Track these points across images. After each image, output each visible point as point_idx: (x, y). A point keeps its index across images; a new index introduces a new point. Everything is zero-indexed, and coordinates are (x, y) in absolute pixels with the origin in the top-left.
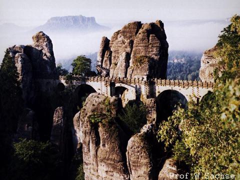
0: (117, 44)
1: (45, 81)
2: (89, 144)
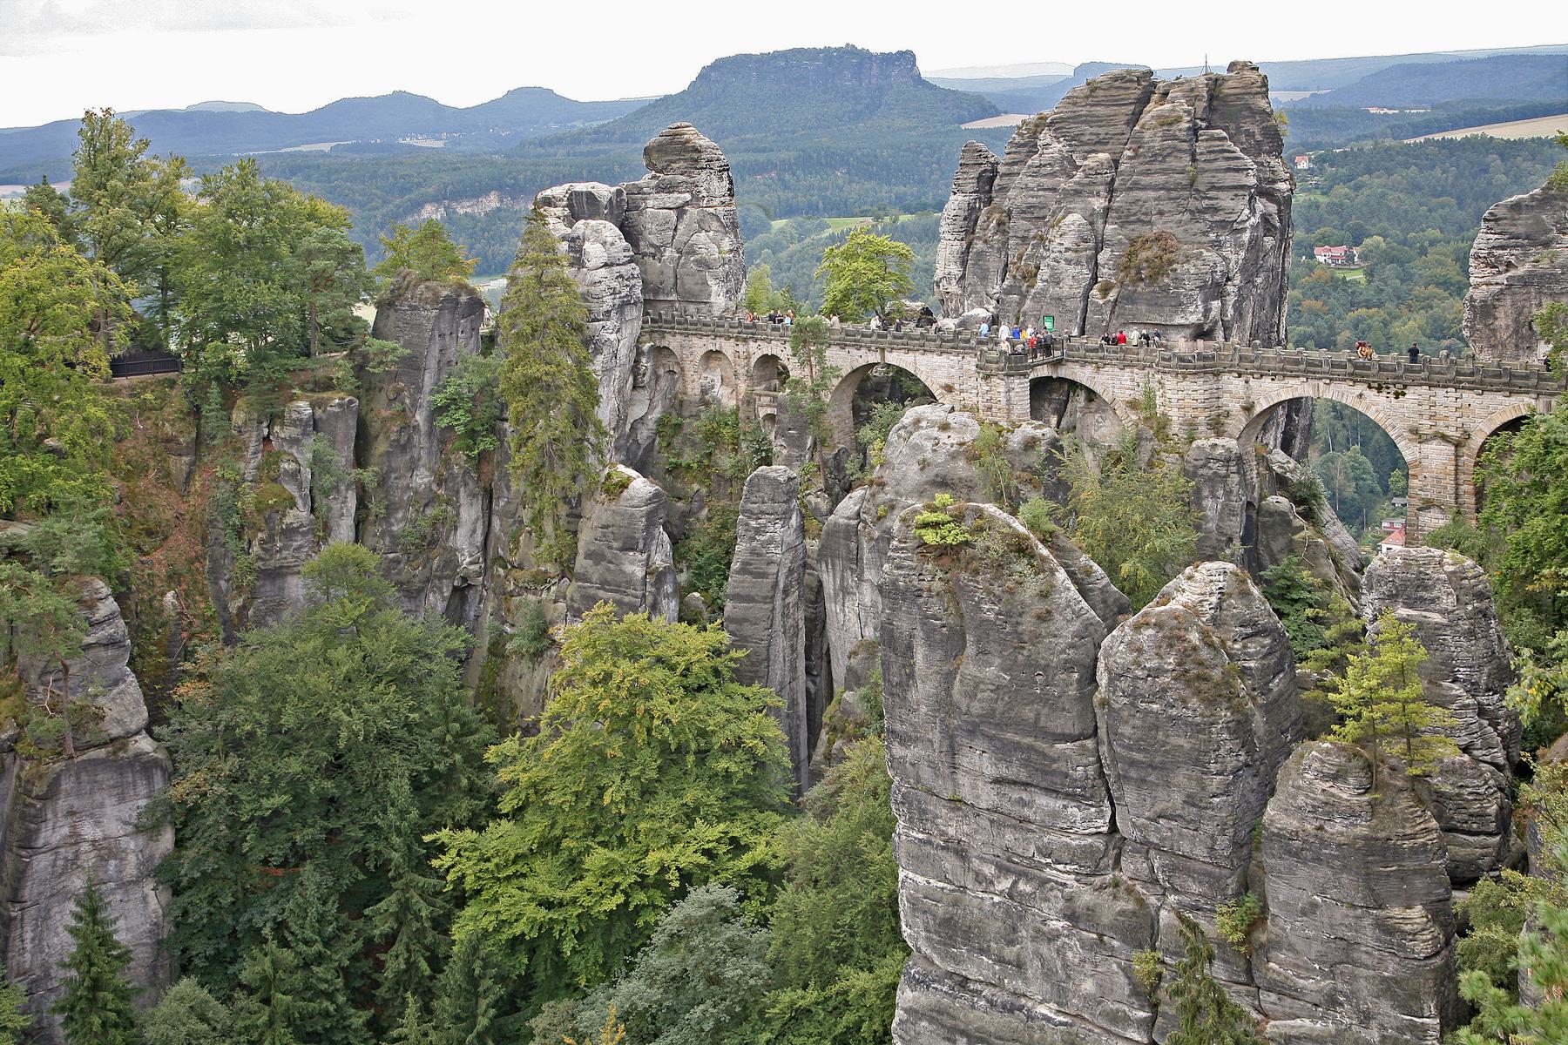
1: (700, 345)
2: (910, 648)
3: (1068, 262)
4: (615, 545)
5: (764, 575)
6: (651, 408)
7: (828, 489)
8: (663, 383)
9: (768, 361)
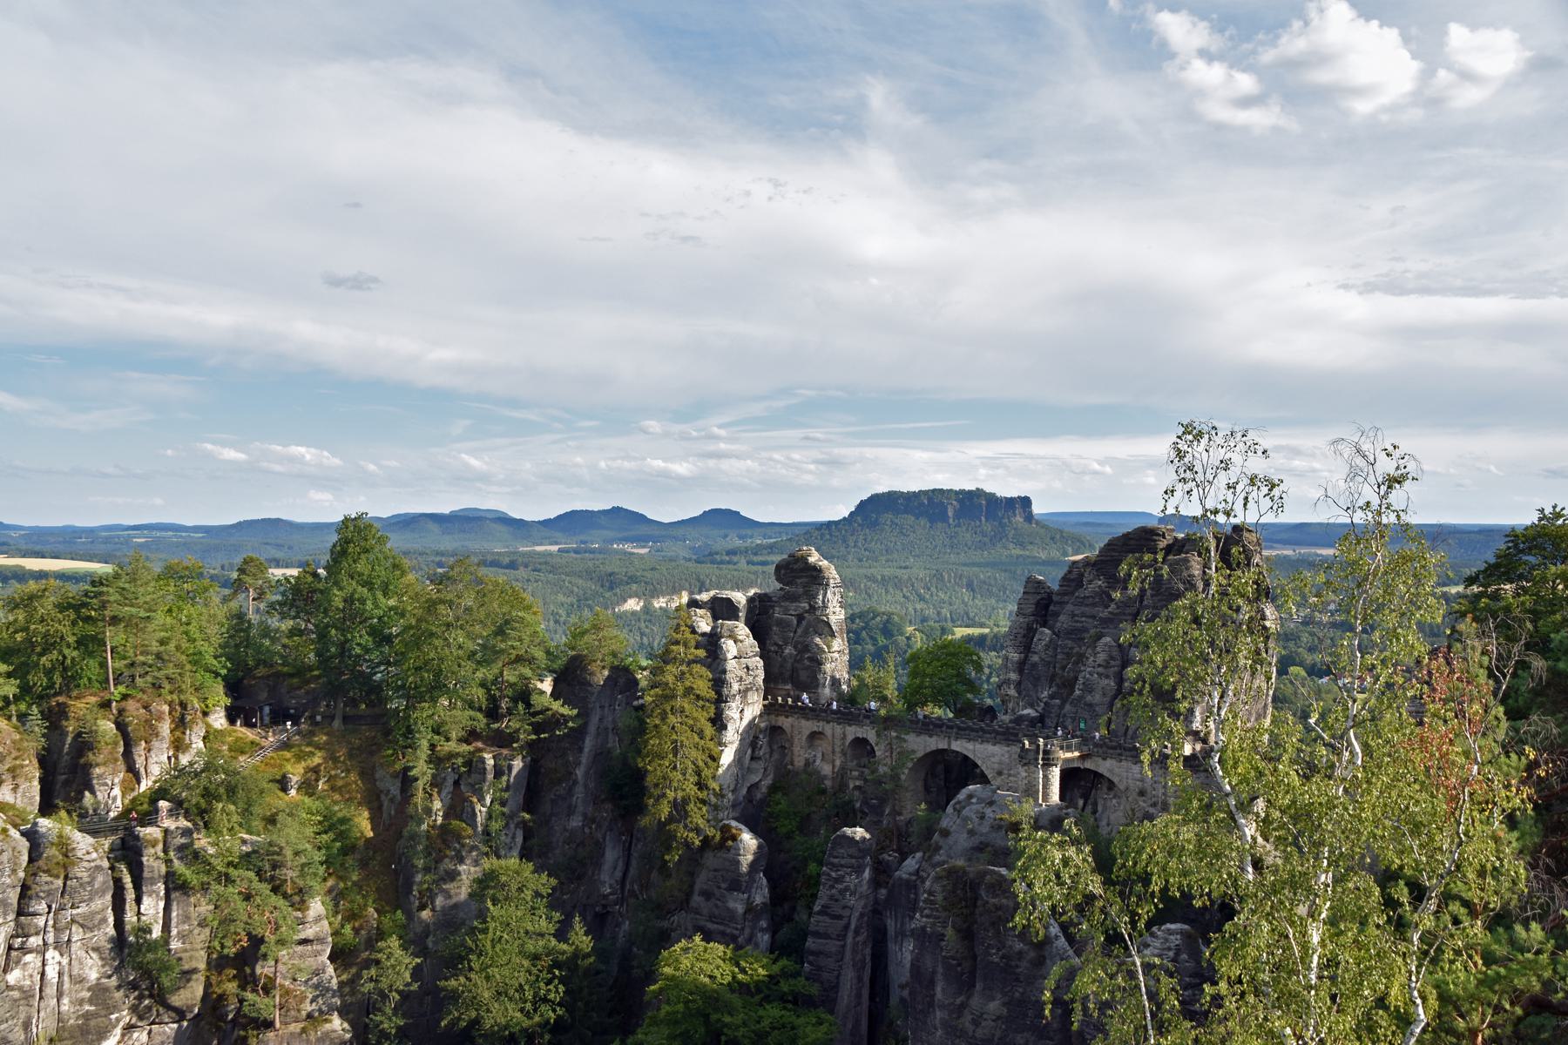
0: (1081, 604)
1: (808, 726)
3: (1100, 675)
4: (723, 886)
5: (840, 917)
6: (765, 775)
7: (899, 850)
8: (776, 756)
9: (860, 743)
